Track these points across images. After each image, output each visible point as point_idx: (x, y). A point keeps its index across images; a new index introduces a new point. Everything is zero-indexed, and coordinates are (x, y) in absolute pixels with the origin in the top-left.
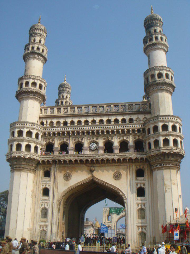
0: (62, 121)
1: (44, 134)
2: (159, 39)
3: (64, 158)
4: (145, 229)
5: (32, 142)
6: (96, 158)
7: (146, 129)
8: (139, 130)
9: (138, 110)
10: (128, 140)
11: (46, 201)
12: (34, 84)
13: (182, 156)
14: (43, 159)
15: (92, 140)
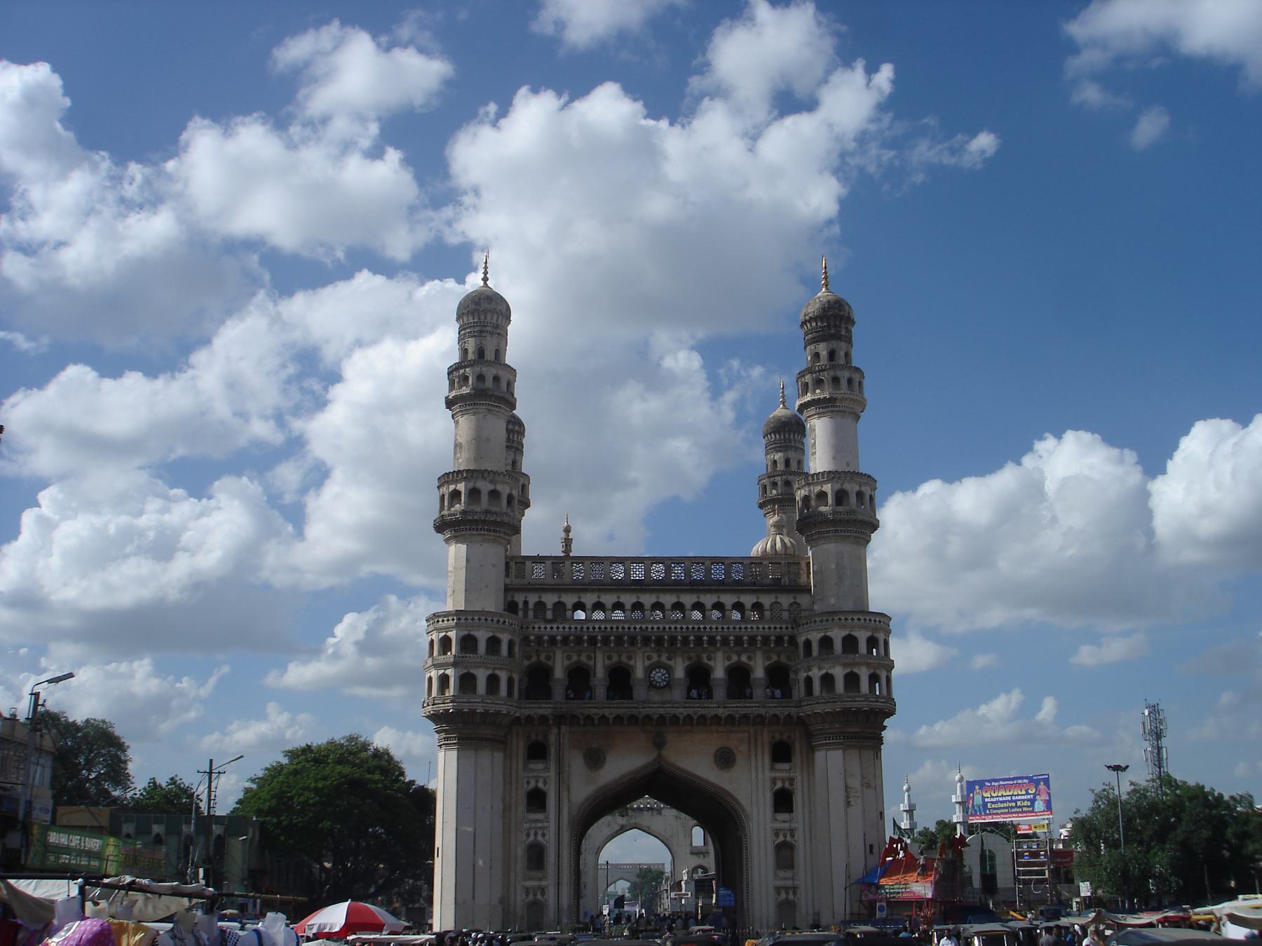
0: (569, 600)
1: (526, 640)
2: (844, 383)
3: (586, 712)
4: (795, 893)
5: (501, 669)
6: (672, 711)
7: (801, 640)
8: (779, 639)
9: (777, 582)
10: (751, 663)
11: (540, 825)
12: (494, 494)
13: (891, 713)
14: (527, 712)
15: (655, 658)
